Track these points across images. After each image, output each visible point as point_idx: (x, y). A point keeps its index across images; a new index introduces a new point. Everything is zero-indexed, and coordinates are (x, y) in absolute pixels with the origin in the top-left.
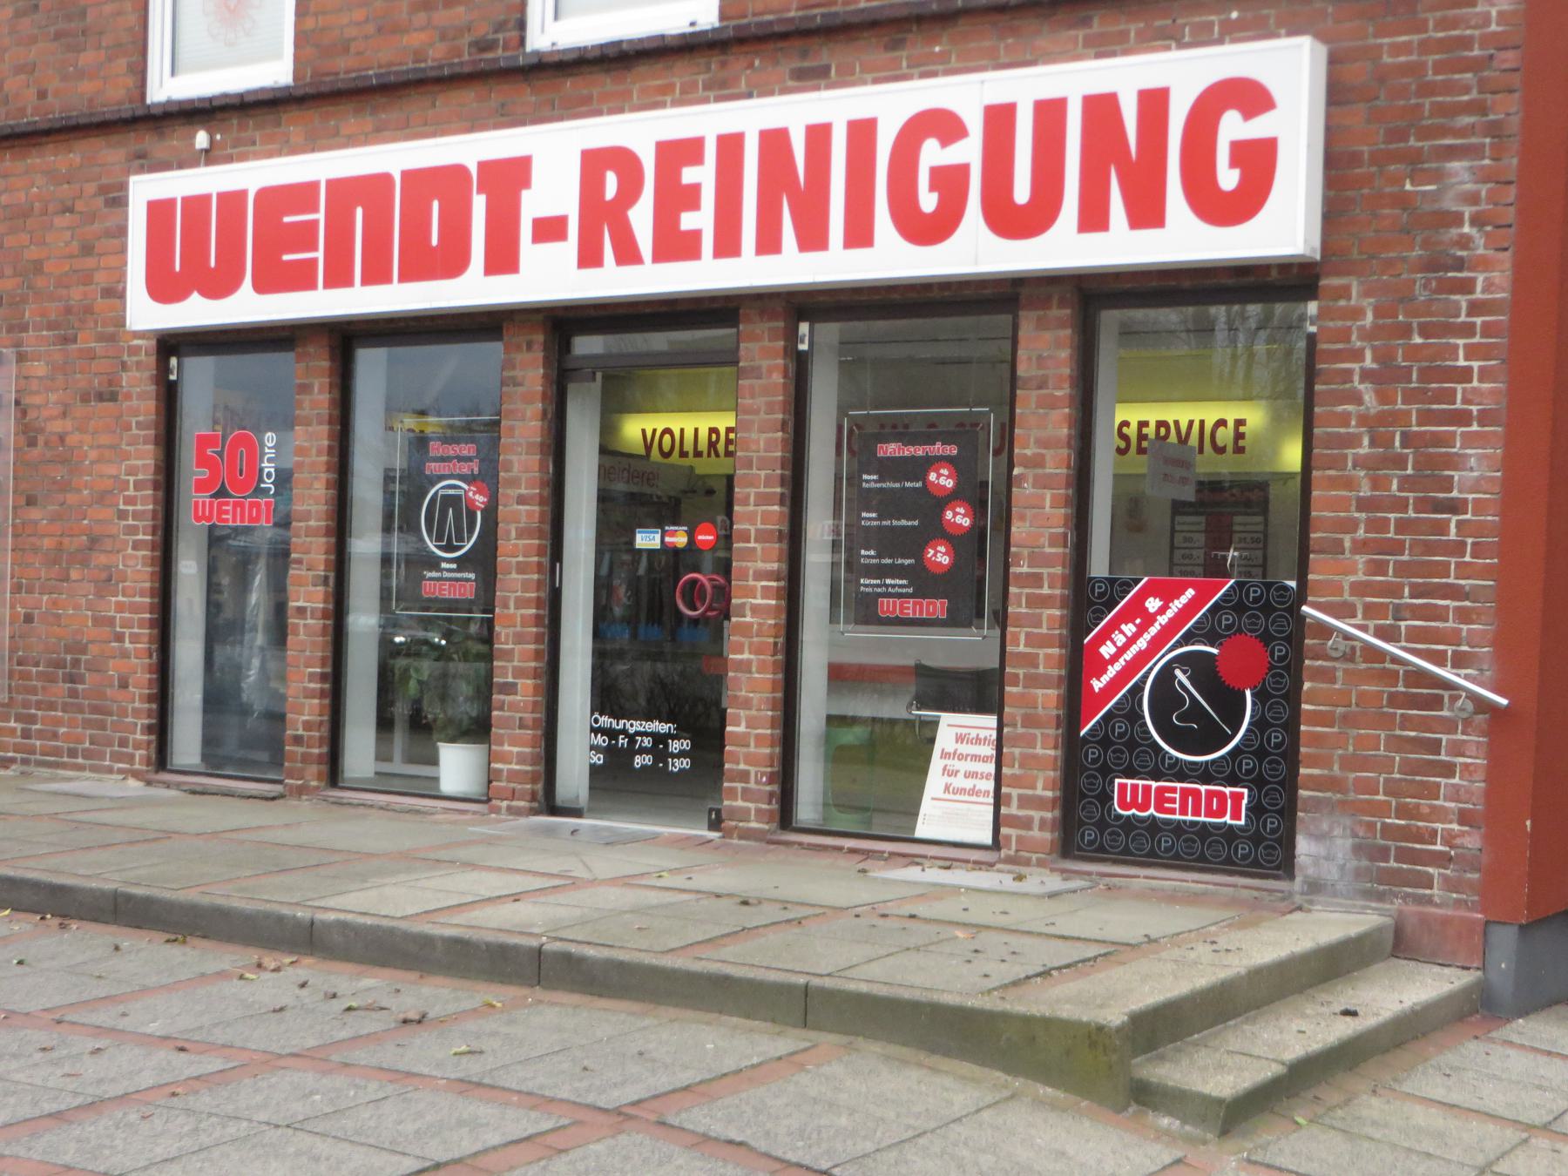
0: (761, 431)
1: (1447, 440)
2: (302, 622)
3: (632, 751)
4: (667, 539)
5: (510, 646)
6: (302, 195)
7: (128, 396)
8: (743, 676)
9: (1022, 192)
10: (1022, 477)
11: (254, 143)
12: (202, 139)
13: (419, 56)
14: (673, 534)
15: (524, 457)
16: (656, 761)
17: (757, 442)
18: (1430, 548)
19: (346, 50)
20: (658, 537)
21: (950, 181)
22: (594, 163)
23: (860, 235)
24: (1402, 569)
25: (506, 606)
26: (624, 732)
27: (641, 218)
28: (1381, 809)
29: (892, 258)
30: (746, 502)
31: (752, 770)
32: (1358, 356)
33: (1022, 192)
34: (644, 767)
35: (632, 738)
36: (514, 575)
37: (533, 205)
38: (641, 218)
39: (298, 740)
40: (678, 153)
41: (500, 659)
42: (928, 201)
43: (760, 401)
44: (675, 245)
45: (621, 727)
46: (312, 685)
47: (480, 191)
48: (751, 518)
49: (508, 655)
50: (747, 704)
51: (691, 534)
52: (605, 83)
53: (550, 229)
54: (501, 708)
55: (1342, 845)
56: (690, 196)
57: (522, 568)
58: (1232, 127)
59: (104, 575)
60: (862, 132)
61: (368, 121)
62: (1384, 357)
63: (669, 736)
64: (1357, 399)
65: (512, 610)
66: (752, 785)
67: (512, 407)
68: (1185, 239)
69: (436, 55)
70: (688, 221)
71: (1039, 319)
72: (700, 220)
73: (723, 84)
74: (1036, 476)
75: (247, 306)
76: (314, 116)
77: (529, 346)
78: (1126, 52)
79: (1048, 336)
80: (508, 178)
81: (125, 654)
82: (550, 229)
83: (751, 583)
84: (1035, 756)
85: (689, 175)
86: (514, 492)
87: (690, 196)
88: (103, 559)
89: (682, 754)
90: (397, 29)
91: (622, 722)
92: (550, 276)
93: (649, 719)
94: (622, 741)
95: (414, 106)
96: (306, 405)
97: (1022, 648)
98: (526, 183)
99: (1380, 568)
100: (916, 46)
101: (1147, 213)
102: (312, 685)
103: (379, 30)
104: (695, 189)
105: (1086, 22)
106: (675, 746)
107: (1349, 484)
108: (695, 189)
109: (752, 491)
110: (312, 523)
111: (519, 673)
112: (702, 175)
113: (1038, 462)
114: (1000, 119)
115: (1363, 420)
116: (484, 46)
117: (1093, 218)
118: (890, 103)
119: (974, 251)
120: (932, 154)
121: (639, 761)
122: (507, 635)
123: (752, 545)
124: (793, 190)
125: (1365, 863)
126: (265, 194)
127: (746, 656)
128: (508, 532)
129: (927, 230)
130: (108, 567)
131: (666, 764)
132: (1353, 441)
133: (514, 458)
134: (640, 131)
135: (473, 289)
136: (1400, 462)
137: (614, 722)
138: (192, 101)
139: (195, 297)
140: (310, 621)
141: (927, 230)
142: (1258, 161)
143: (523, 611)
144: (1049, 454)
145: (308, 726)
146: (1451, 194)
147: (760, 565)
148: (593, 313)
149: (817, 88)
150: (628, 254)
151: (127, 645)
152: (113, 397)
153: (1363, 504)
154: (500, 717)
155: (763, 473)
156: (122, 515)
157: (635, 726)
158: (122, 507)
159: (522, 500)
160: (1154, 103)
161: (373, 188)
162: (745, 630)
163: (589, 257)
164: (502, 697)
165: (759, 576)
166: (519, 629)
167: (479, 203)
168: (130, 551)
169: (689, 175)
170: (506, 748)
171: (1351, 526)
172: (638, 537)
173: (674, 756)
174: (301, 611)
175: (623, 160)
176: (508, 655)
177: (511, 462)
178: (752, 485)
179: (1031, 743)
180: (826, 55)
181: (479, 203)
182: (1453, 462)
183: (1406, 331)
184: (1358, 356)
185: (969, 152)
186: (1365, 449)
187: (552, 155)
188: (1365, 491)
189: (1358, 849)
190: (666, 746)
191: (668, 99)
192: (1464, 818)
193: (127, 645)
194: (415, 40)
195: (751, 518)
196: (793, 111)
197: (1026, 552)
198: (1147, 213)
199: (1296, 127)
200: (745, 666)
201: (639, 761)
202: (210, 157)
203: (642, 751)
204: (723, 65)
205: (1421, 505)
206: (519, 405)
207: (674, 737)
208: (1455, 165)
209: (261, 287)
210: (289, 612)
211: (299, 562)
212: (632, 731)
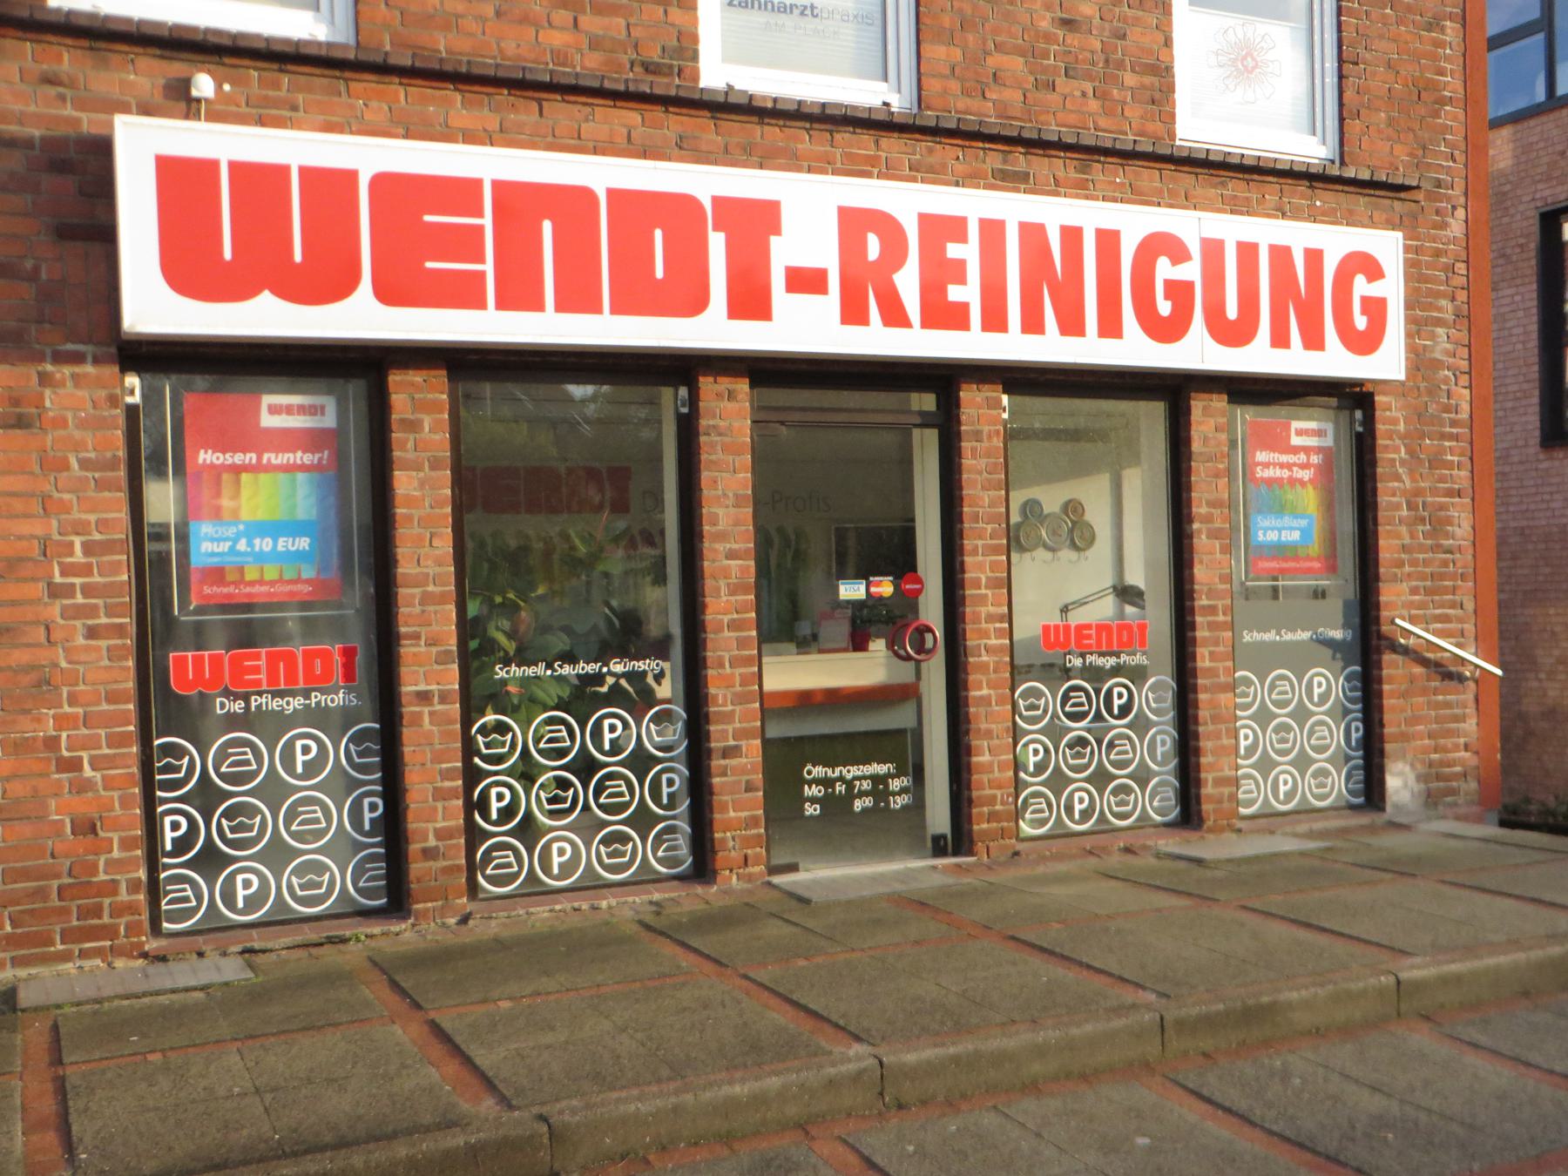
0: (983, 488)
1: (1442, 507)
2: (426, 710)
3: (851, 795)
4: (873, 589)
5: (730, 708)
6: (462, 193)
7: (61, 423)
8: (982, 710)
9: (1232, 312)
10: (1200, 531)
11: (295, 108)
12: (204, 85)
13: (560, 56)
14: (878, 584)
15: (732, 510)
16: (876, 803)
17: (982, 499)
18: (1442, 577)
19: (446, 27)
20: (863, 588)
21: (1181, 292)
22: (853, 223)
23: (1111, 327)
24: (1428, 591)
25: (722, 665)
26: (841, 779)
27: (908, 283)
28: (1426, 751)
29: (1135, 350)
30: (975, 552)
31: (998, 793)
32: (1397, 450)
33: (1232, 312)
34: (865, 810)
35: (850, 784)
36: (726, 633)
37: (785, 253)
38: (908, 283)
39: (428, 854)
40: (941, 229)
41: (718, 722)
42: (1164, 308)
43: (982, 463)
44: (943, 315)
45: (837, 774)
46: (447, 784)
47: (716, 229)
48: (981, 567)
49: (727, 718)
50: (989, 734)
51: (897, 587)
52: (804, 140)
53: (806, 281)
54: (725, 774)
55: (1411, 777)
56: (958, 272)
57: (733, 625)
58: (1361, 287)
59: (26, 680)
60: (1108, 241)
61: (492, 121)
62: (1410, 452)
63: (889, 776)
64: (1398, 478)
65: (728, 670)
66: (998, 807)
67: (713, 457)
68: (1335, 362)
69: (587, 65)
70: (955, 293)
71: (1204, 408)
72: (967, 293)
73: (931, 170)
74: (1209, 530)
75: (358, 317)
76: (401, 94)
77: (731, 396)
78: (1248, 213)
79: (1212, 422)
80: (753, 223)
81: (82, 787)
82: (806, 281)
83: (984, 625)
84: (1223, 747)
85: (954, 250)
86: (721, 547)
87: (958, 272)
88: (20, 657)
89: (903, 791)
90: (525, 19)
91: (837, 770)
92: (805, 327)
93: (867, 762)
94: (840, 788)
95: (562, 112)
96: (410, 445)
97: (1207, 664)
98: (778, 233)
99: (1414, 591)
100: (1099, 171)
101: (1314, 341)
102: (447, 784)
103: (498, 14)
104: (961, 264)
105: (1223, 184)
106: (895, 785)
107: (1399, 536)
108: (961, 264)
109: (980, 543)
110: (431, 588)
111: (739, 734)
112: (967, 252)
113: (1208, 519)
114: (1213, 250)
115: (1404, 492)
116: (650, 68)
117: (1280, 339)
118: (1135, 222)
119: (1197, 352)
120: (1165, 270)
121: (858, 805)
122: (725, 696)
123: (983, 591)
124: (1052, 282)
125: (1422, 786)
126: (382, 182)
127: (985, 692)
128: (718, 589)
129: (1167, 330)
130: (33, 667)
131: (888, 803)
132: (1398, 507)
133: (721, 512)
134: (907, 201)
135: (712, 330)
136: (1423, 520)
137: (830, 771)
138: (195, 29)
139: (266, 297)
140: (439, 707)
141: (1167, 330)
142: (1375, 308)
143: (742, 670)
144: (1216, 512)
145: (441, 835)
146: (1438, 348)
147: (991, 609)
148: (804, 367)
149: (1017, 190)
150: (895, 316)
151: (88, 772)
152: (21, 423)
153: (1404, 548)
154: (723, 784)
155: (989, 527)
156: (55, 592)
157: (852, 772)
158: (58, 579)
159: (731, 555)
160: (1314, 258)
161: (571, 204)
162: (983, 668)
163: (853, 313)
164: (723, 762)
165: (991, 618)
166: (738, 689)
167: (717, 243)
168: (81, 641)
169: (954, 250)
170: (732, 814)
171: (1400, 564)
172: (842, 589)
173: (894, 794)
174: (424, 697)
175: (886, 225)
176: (727, 718)
177: (716, 515)
178: (980, 538)
179: (1219, 737)
180: (1020, 160)
181: (717, 243)
182: (1449, 521)
183: (1422, 436)
184: (1397, 450)
185: (1191, 271)
186: (1405, 513)
187: (810, 210)
188: (1407, 541)
189: (1419, 778)
190: (887, 786)
191: (876, 171)
192: (1466, 747)
193: (88, 772)
194: (557, 39)
195: (981, 567)
196: (1055, 212)
197: (1205, 589)
198: (1314, 341)
199: (1392, 289)
200: (986, 701)
201: (858, 805)
202: (217, 115)
203: (862, 794)
204: (930, 151)
205: (1433, 549)
206: (718, 455)
207: (893, 777)
208: (1440, 331)
209: (388, 293)
210: (404, 700)
211: (417, 636)
212: (849, 777)
